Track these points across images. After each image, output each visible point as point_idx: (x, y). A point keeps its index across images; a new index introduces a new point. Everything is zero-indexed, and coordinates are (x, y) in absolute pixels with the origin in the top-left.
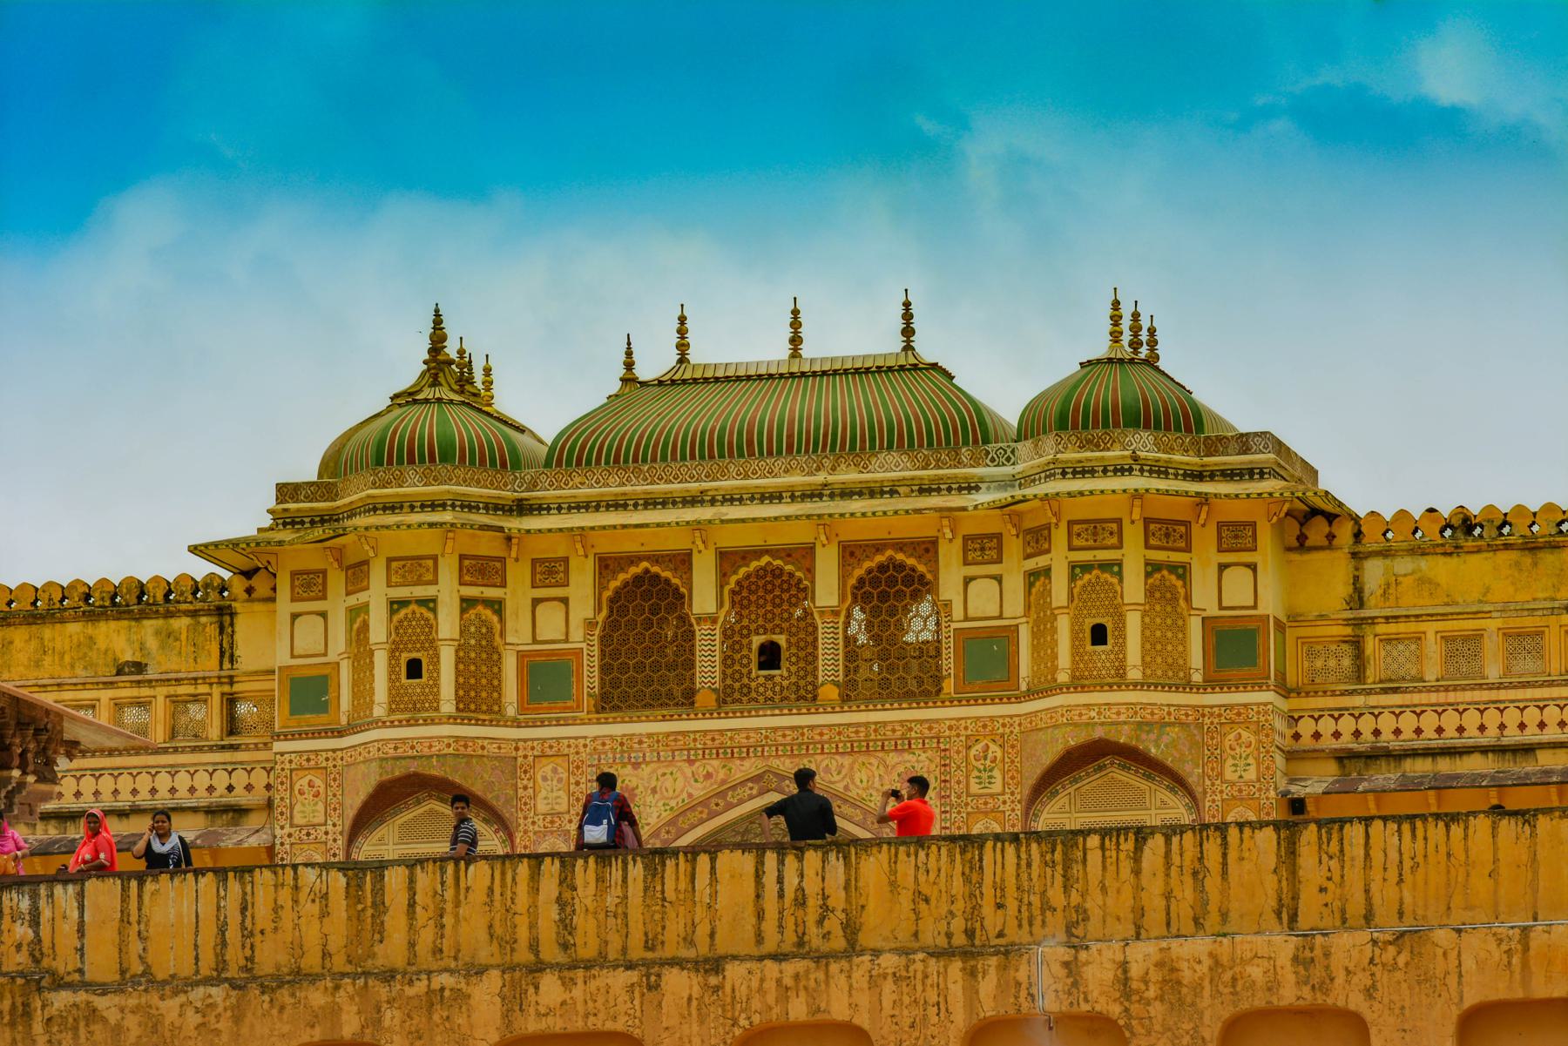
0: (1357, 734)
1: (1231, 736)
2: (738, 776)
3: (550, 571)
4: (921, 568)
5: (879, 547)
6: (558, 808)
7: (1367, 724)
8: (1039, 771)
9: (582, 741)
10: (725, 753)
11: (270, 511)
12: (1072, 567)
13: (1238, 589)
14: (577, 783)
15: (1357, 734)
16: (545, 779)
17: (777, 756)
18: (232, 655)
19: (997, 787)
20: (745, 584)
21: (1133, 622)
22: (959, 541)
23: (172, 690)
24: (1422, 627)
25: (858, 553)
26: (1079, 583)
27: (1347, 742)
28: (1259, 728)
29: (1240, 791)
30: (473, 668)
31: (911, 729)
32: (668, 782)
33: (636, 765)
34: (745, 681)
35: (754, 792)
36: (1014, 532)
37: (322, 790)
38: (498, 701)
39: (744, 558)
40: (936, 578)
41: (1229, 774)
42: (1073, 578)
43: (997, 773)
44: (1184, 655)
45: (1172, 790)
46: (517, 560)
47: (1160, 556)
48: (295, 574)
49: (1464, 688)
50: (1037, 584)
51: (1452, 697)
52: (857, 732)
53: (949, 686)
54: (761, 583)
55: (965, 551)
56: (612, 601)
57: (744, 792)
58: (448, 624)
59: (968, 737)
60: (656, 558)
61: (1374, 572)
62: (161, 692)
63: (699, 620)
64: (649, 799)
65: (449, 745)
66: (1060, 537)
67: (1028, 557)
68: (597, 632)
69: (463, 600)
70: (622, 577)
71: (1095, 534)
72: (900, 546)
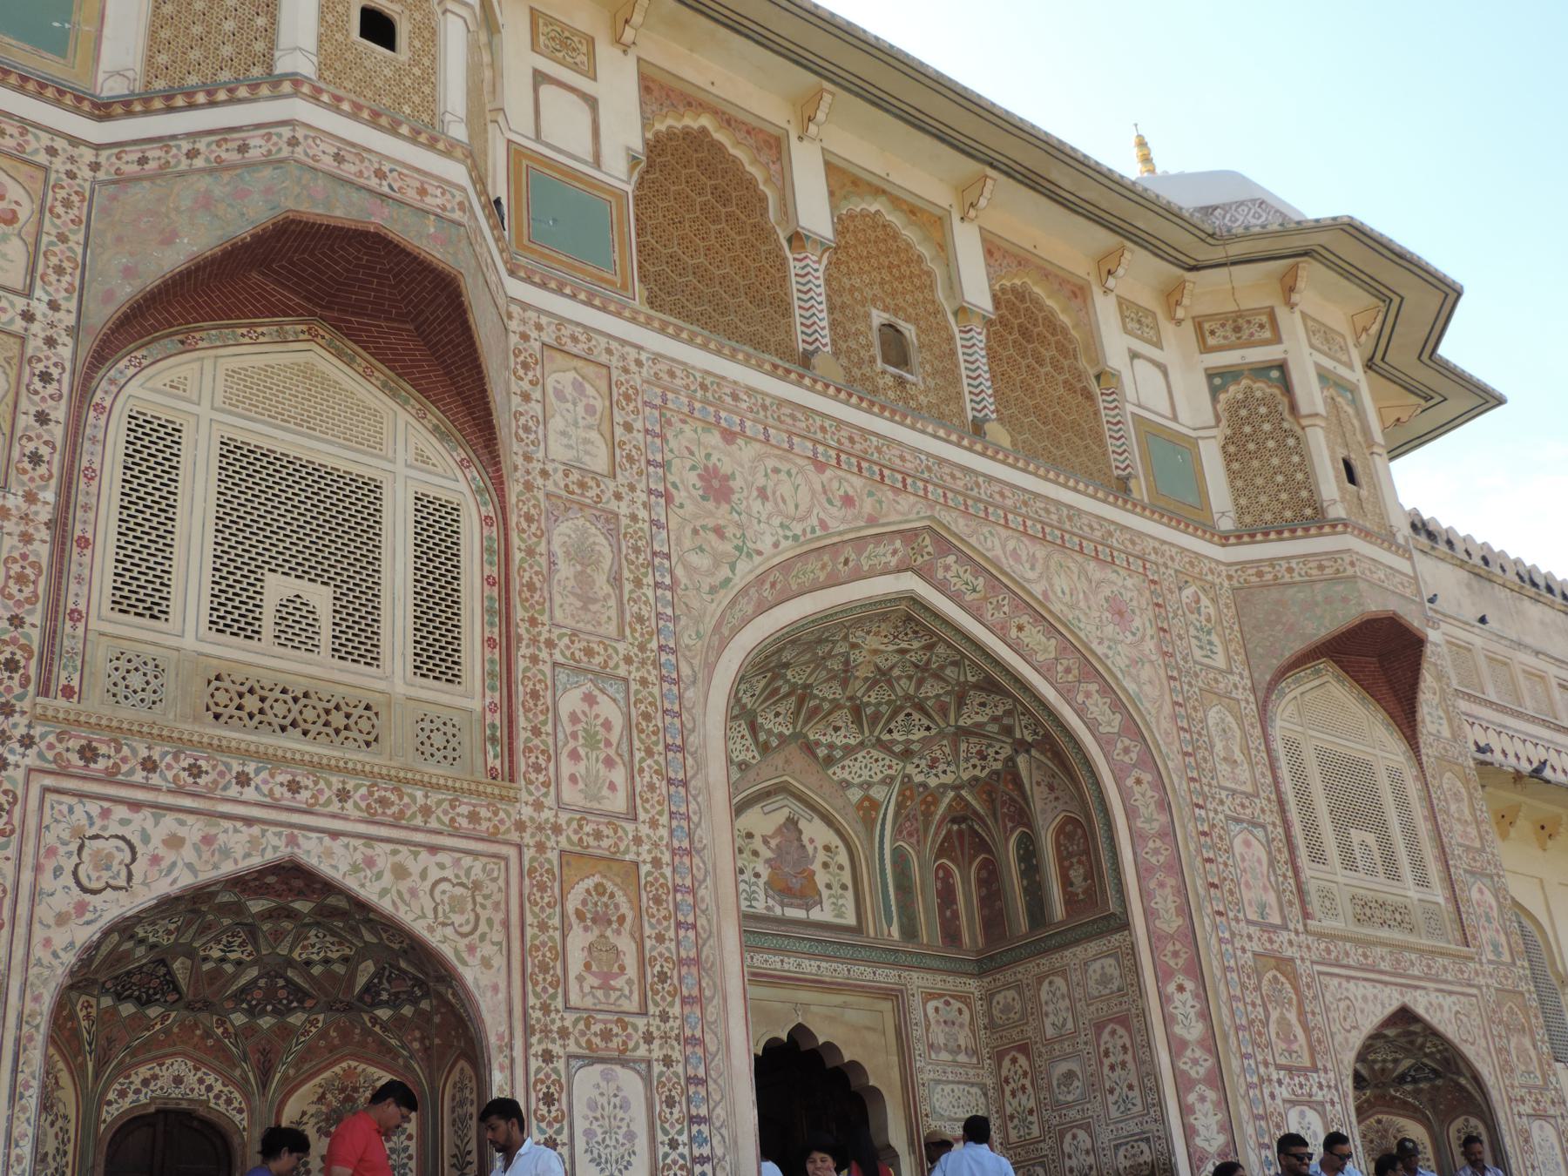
4: (1065, 319)
14: (628, 427)
22: (1112, 298)
33: (729, 436)
34: (866, 370)
35: (894, 561)
37: (24, 213)
50: (1232, 389)
60: (729, 122)
64: (757, 506)
67: (1205, 349)
70: (670, 122)
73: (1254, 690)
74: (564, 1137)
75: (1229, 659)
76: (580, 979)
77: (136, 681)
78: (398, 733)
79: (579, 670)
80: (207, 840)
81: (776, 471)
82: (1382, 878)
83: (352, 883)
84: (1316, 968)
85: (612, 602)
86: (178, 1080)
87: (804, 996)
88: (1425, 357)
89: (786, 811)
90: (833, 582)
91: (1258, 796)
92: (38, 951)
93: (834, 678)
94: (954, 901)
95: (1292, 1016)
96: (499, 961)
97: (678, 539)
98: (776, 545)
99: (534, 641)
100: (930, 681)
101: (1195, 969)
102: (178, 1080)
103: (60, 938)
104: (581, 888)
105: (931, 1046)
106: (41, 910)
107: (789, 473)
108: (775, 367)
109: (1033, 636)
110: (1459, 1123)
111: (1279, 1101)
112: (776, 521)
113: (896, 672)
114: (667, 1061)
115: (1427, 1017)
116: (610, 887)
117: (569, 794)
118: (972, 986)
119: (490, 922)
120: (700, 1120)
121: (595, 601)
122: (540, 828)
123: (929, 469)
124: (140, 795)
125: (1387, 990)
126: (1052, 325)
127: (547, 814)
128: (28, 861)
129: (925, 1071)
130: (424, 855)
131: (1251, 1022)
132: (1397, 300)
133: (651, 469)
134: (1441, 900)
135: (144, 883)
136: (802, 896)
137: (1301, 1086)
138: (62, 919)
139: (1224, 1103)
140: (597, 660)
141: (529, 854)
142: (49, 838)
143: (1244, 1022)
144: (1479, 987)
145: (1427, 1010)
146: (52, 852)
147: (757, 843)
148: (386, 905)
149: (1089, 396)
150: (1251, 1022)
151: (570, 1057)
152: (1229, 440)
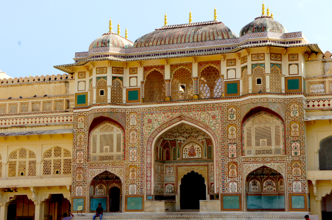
0: (324, 105)
1: (292, 106)
2: (175, 116)
3: (133, 71)
4: (217, 68)
5: (207, 63)
8: (245, 115)
9: (140, 109)
10: (172, 111)
11: (73, 59)
12: (252, 65)
13: (294, 70)
14: (139, 118)
16: (132, 118)
18: (68, 92)
19: (235, 119)
20: (177, 72)
22: (226, 61)
23: (56, 99)
26: (254, 69)
27: (321, 107)
28: (299, 104)
29: (295, 119)
30: (115, 92)
31: (214, 105)
33: (152, 114)
35: (179, 120)
36: (239, 58)
37: (84, 121)
38: (122, 100)
39: (176, 66)
40: (220, 70)
41: (292, 115)
42: (252, 68)
43: (235, 115)
44: (280, 86)
46: (126, 68)
50: (244, 70)
52: (202, 106)
55: (227, 63)
56: (147, 77)
57: (176, 120)
59: (227, 106)
60: (157, 67)
62: (53, 99)
63: (166, 80)
64: (155, 122)
65: (109, 110)
66: (249, 58)
67: (242, 64)
68: (144, 84)
69: (113, 77)
70: (149, 72)
71: (258, 57)
72: (212, 62)
73: (240, 122)
76: (131, 177)
80: (100, 170)
81: (158, 116)
82: (266, 146)
83: (111, 172)
84: (242, 163)
86: (114, 185)
87: (193, 167)
89: (192, 144)
92: (89, 180)
93: (187, 130)
95: (235, 170)
96: (123, 176)
97: (144, 130)
98: (157, 126)
99: (127, 146)
102: (114, 185)
103: (90, 179)
104: (131, 169)
106: (89, 178)
107: (160, 116)
109: (200, 124)
111: (228, 182)
112: (157, 123)
114: (139, 184)
115: (270, 167)
116: (134, 168)
117: (131, 160)
122: (127, 164)
123: (181, 107)
124: (95, 168)
125: (260, 164)
128: (88, 174)
130: (117, 168)
131: (225, 172)
133: (141, 122)
134: (282, 147)
136: (193, 155)
138: (90, 178)
140: (134, 146)
141: (126, 166)
142: (89, 172)
143: (224, 172)
145: (270, 166)
146: (89, 173)
147: (187, 150)
148: (114, 173)
150: (225, 172)
152: (244, 79)
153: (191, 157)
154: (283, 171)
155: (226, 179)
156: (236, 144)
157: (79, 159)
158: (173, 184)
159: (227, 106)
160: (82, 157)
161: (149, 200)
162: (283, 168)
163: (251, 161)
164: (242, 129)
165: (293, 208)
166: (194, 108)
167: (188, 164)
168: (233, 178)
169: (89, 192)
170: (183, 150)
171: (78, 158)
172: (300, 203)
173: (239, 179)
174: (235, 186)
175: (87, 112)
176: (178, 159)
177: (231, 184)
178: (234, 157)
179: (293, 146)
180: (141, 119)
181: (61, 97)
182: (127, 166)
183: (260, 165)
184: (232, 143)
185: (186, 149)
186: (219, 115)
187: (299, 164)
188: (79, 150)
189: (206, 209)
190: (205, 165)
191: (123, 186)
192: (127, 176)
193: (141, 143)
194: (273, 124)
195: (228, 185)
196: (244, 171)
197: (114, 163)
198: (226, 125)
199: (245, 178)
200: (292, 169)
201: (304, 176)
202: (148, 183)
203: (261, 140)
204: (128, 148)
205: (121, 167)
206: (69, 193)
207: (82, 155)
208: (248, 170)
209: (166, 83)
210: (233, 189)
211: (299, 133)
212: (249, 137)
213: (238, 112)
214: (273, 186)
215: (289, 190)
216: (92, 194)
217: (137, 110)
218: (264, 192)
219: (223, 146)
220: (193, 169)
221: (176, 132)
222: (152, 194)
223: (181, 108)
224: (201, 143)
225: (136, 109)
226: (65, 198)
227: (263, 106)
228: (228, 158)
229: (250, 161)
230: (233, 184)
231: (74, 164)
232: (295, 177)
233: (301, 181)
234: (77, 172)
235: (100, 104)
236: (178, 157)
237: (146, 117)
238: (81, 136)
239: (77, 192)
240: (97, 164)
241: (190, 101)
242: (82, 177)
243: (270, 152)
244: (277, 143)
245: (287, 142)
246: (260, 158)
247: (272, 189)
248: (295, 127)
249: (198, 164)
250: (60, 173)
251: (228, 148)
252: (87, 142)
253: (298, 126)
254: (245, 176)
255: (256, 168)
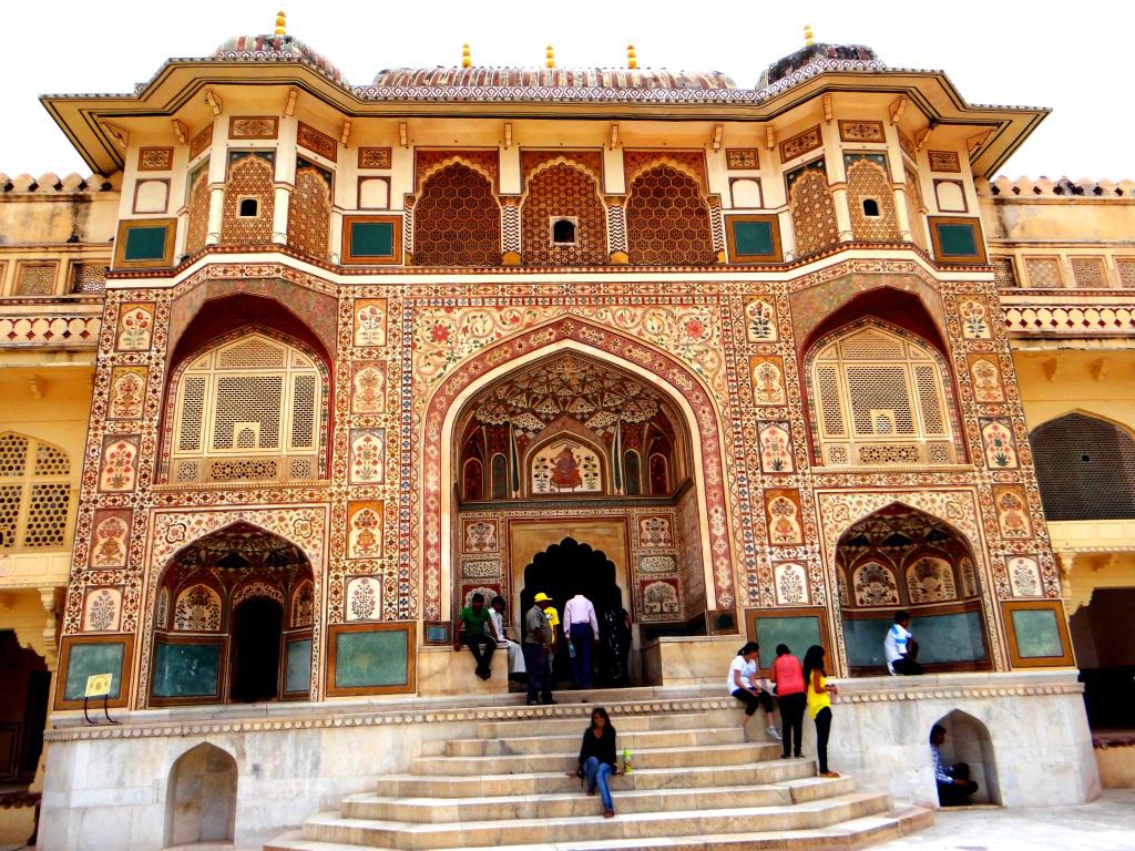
1: (965, 305)
3: (376, 157)
4: (690, 173)
5: (656, 155)
6: (375, 342)
7: (1029, 317)
8: (819, 319)
10: (530, 302)
13: (950, 200)
14: (395, 322)
15: (1024, 323)
16: (363, 318)
17: (577, 305)
20: (542, 178)
21: (900, 198)
22: (722, 154)
23: (25, 256)
24: (1056, 251)
25: (638, 158)
26: (850, 168)
28: (987, 300)
29: (980, 347)
30: (304, 217)
31: (694, 289)
32: (479, 324)
33: (449, 309)
34: (544, 249)
35: (553, 337)
39: (542, 157)
41: (968, 334)
42: (847, 164)
45: (922, 344)
47: (907, 157)
48: (143, 151)
49: (1098, 294)
50: (799, 179)
51: (1090, 300)
53: (724, 257)
54: (555, 178)
55: (728, 159)
56: (424, 183)
58: (285, 169)
60: (466, 155)
61: (1009, 211)
63: (504, 199)
64: (461, 337)
65: (278, 271)
68: (414, 207)
70: (437, 167)
73: (794, 348)
74: (342, 605)
75: (779, 334)
76: (355, 547)
77: (187, 472)
78: (281, 470)
79: (361, 430)
80: (211, 520)
81: (475, 317)
82: (895, 433)
83: (263, 526)
84: (816, 491)
85: (382, 398)
86: (258, 590)
88: (962, 108)
90: (515, 356)
91: (787, 406)
92: (155, 564)
94: (664, 472)
95: (792, 519)
96: (320, 545)
97: (418, 363)
99: (342, 423)
100: (606, 383)
101: (723, 502)
102: (258, 590)
103: (161, 559)
104: (357, 515)
105: (642, 541)
106: (156, 551)
107: (481, 317)
108: (475, 269)
109: (637, 353)
110: (963, 562)
111: (769, 562)
112: (472, 341)
113: (589, 380)
116: (371, 511)
117: (355, 479)
118: (672, 510)
119: (317, 532)
120: (404, 595)
121: (371, 400)
123: (567, 290)
126: (681, 180)
127: (344, 488)
129: (636, 552)
130: (292, 512)
131: (754, 525)
132: (913, 89)
134: (951, 439)
135: (189, 537)
137: (789, 553)
138: (162, 553)
139: (730, 566)
140: (371, 423)
141: (333, 505)
142: (158, 528)
143: (749, 525)
144: (976, 486)
145: (918, 503)
146: (159, 532)
147: (548, 463)
148: (276, 532)
149: (703, 213)
150: (754, 525)
151: (346, 577)
153: (562, 490)
154: (969, 523)
155: (763, 552)
156: (785, 426)
157: (113, 475)
158: (495, 587)
159: (739, 292)
160: (130, 466)
161: (436, 643)
162: (966, 511)
163: (849, 484)
164: (801, 372)
165: (1023, 655)
166: (617, 297)
167: (554, 513)
168: (788, 546)
169: (150, 616)
170: (533, 466)
171: (110, 470)
172: (1045, 635)
173: (813, 552)
174: (798, 577)
175: (169, 291)
176: (514, 496)
177: (780, 570)
178: (784, 470)
179: (990, 436)
180: (405, 323)
181: (50, 249)
182: (339, 501)
183: (884, 500)
184: (770, 422)
185: (543, 460)
186: (712, 323)
187: (1019, 499)
188: (116, 437)
189: (689, 674)
190: (618, 519)
191: (317, 587)
192: (339, 545)
193: (404, 415)
194: (909, 361)
195: (769, 575)
196: (825, 521)
197: (281, 491)
198: (742, 356)
199: (834, 549)
200: (998, 513)
201: (1042, 539)
202: (428, 572)
203: (874, 414)
204: (347, 433)
205: (312, 508)
206: (51, 622)
207: (129, 455)
208: (839, 519)
209: (501, 207)
210: (793, 592)
211: (1001, 393)
212: (831, 399)
213: (784, 317)
214: (886, 582)
215: (998, 588)
216: (164, 626)
217: (388, 291)
218: (859, 604)
219: (740, 429)
220: (571, 530)
221: (522, 391)
222: (446, 617)
223: (568, 291)
224: (599, 440)
225: (385, 288)
226: (24, 645)
227: (899, 287)
228: (763, 473)
229: (844, 485)
230: (789, 572)
231: (89, 493)
232: (1012, 541)
233: (1034, 558)
234: (101, 527)
235: (239, 248)
236: (516, 490)
237: (424, 319)
238: (130, 381)
239: (93, 615)
240: (199, 491)
241: (601, 270)
242: (123, 549)
243: (913, 454)
244: (933, 424)
245: (966, 420)
246: (882, 476)
247: (885, 594)
248: (986, 374)
249: (590, 512)
250: (12, 541)
251: (759, 440)
252: (159, 406)
253: (995, 370)
254: (833, 539)
255: (871, 509)
